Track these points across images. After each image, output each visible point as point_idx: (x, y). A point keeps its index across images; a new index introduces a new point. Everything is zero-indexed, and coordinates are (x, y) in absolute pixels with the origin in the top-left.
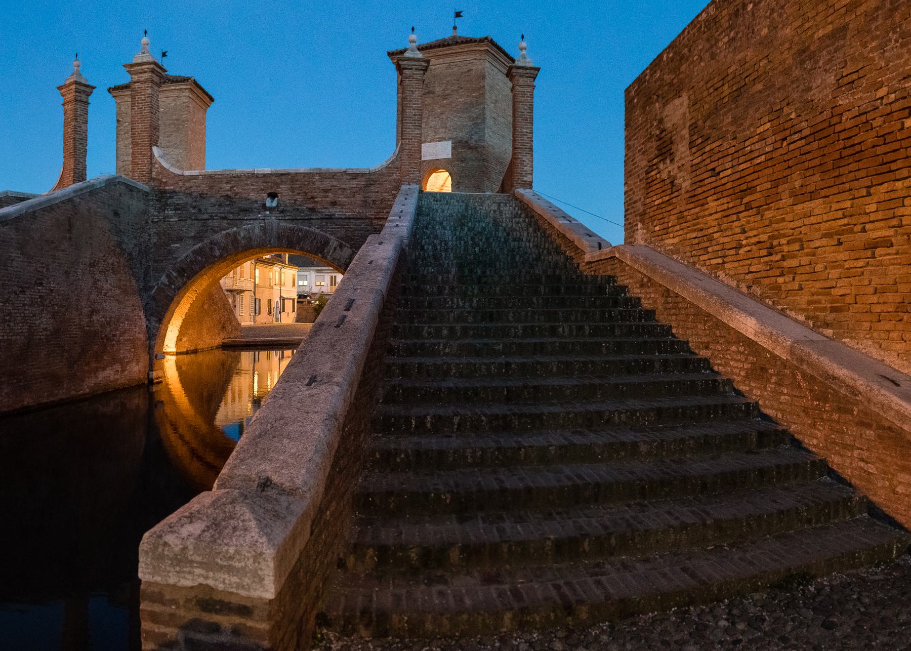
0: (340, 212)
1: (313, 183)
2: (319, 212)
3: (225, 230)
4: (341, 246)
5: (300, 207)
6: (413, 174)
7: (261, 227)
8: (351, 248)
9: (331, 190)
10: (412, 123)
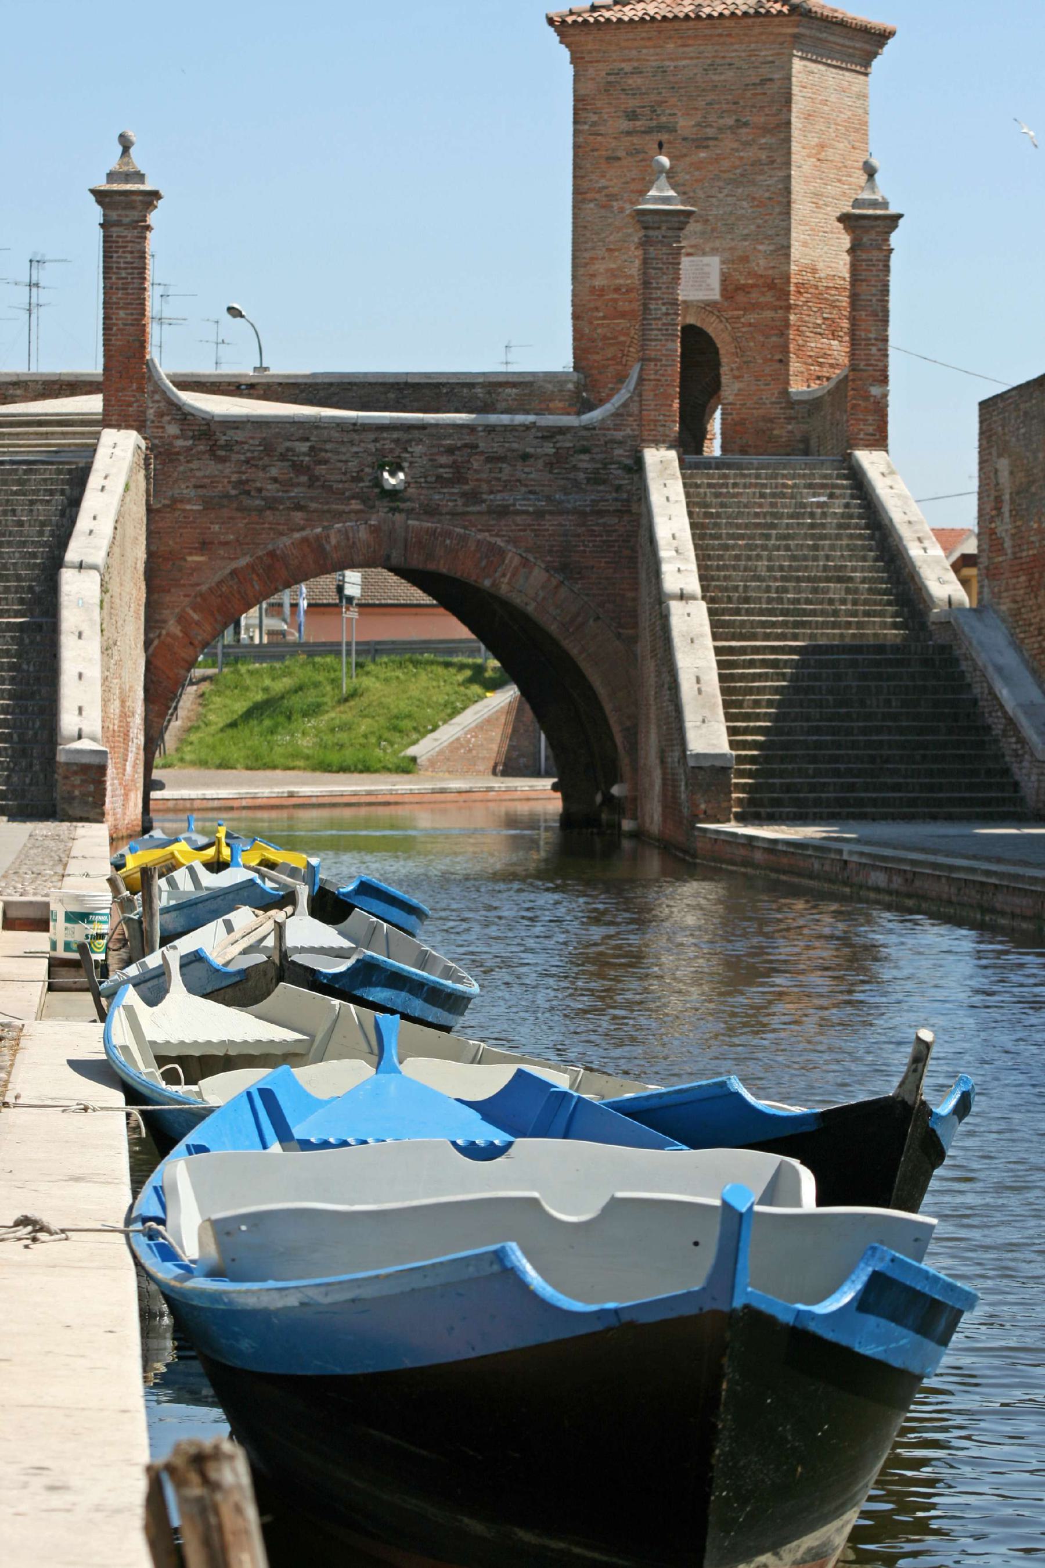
0: (524, 499)
3: (298, 530)
4: (525, 562)
9: (505, 457)
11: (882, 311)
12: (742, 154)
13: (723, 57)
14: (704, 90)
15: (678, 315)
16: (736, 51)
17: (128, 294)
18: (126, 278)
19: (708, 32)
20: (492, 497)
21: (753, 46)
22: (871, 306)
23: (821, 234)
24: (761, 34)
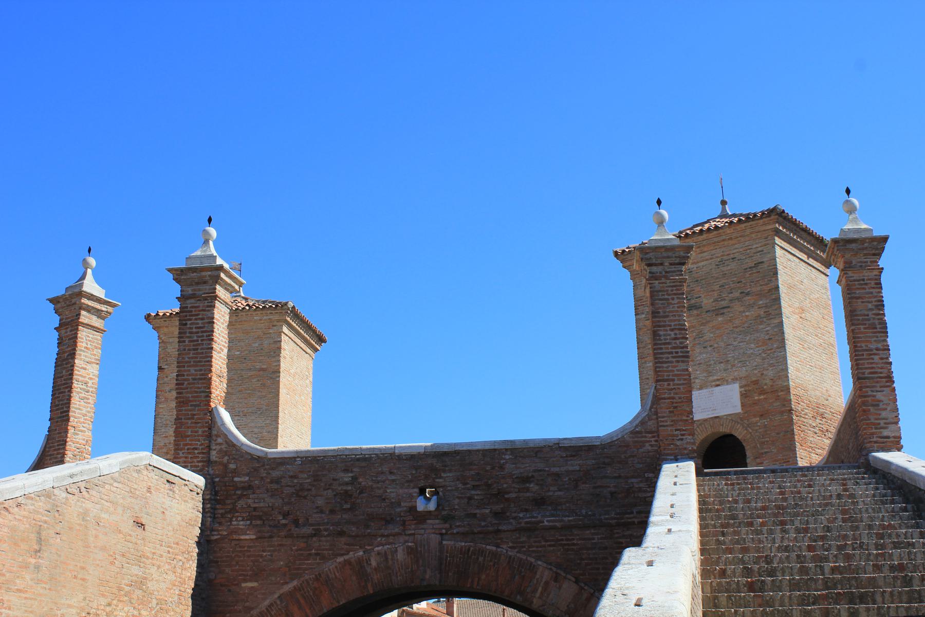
0: (552, 515)
1: (502, 468)
2: (515, 518)
3: (342, 555)
4: (556, 578)
5: (478, 511)
6: (682, 439)
7: (408, 547)
8: (577, 582)
9: (533, 476)
10: (669, 353)
11: (880, 324)
12: (747, 314)
13: (728, 255)
14: (717, 278)
15: (687, 338)
16: (736, 249)
17: (197, 354)
18: (198, 341)
19: (716, 240)
20: (521, 515)
21: (747, 243)
22: (869, 320)
23: (808, 366)
24: (751, 233)
